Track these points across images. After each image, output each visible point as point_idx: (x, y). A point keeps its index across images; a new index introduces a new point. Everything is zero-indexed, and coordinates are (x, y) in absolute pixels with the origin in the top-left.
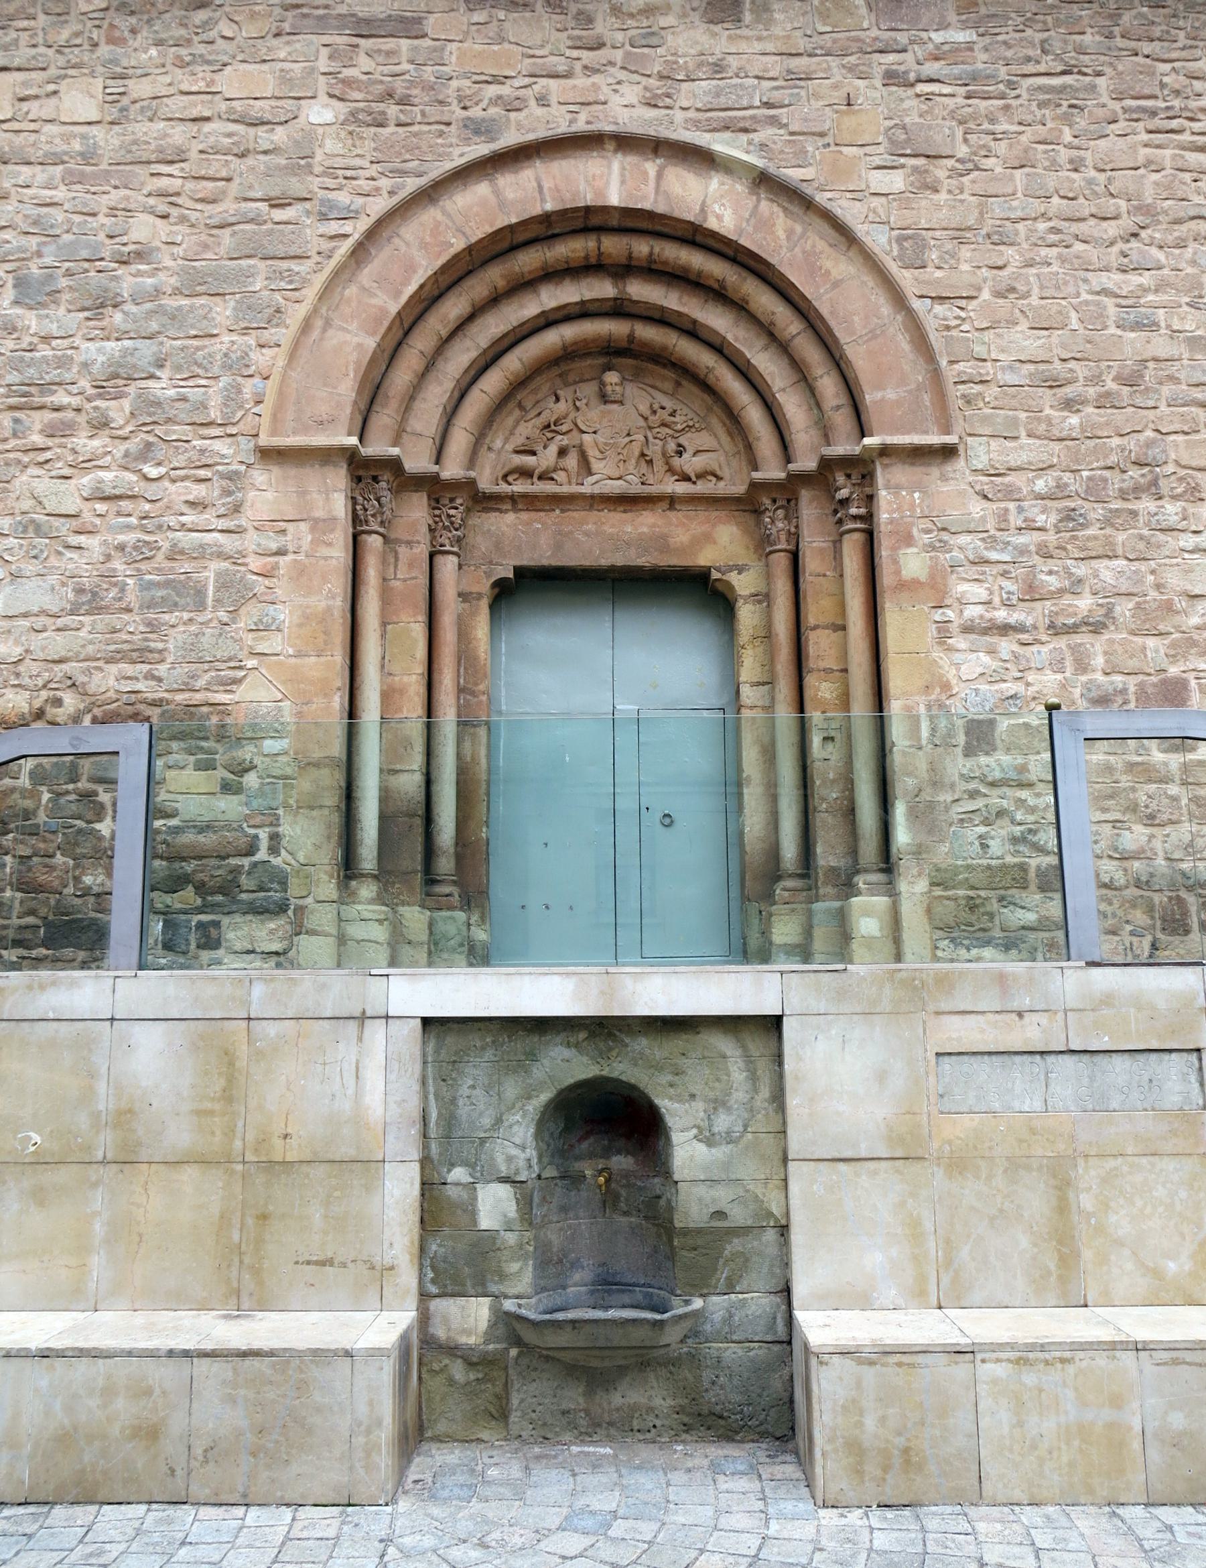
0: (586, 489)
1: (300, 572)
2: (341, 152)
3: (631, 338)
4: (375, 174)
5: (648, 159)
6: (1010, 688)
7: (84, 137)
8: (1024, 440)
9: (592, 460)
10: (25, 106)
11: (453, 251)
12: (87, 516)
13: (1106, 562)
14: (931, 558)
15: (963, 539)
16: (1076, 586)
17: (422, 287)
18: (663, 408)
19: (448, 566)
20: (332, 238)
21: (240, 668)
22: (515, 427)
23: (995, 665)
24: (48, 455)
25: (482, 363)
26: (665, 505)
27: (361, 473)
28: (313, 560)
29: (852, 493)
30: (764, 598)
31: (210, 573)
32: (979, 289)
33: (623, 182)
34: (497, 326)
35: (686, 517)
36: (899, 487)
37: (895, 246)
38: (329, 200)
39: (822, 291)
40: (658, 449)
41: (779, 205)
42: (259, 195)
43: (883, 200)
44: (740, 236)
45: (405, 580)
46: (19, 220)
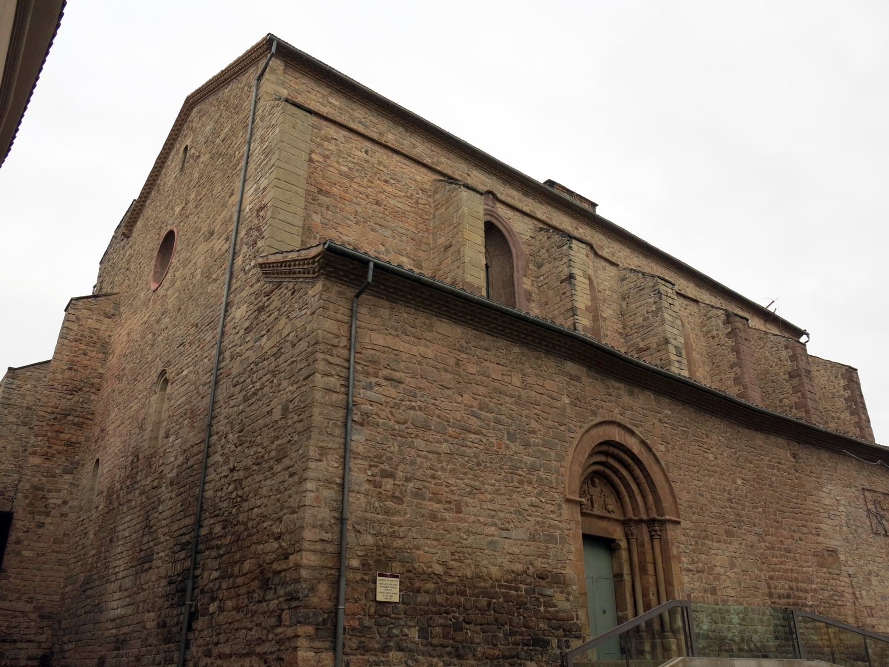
24: (519, 490)
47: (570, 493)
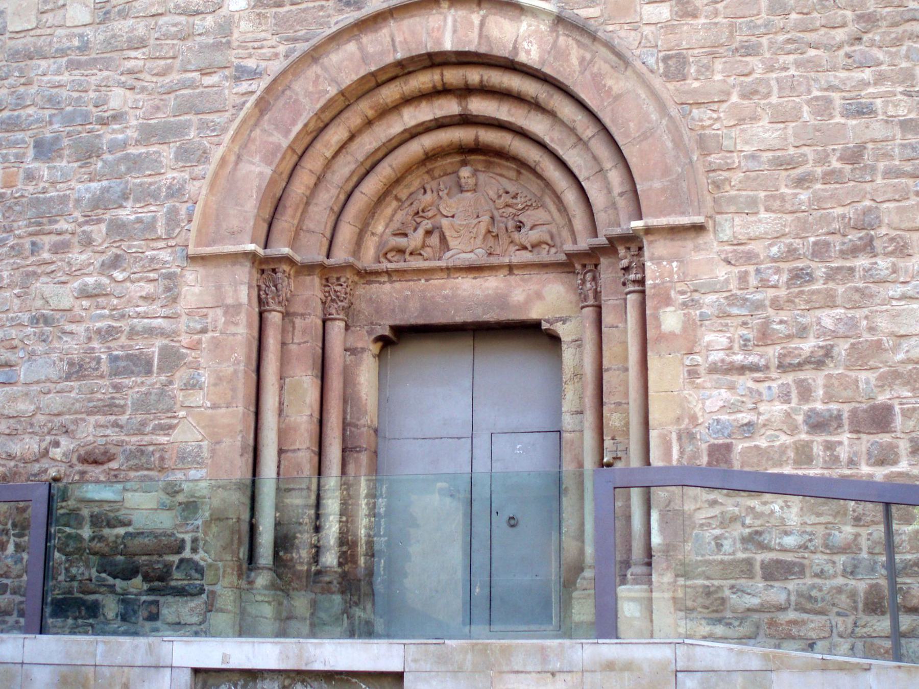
0: (442, 264)
1: (216, 344)
2: (252, 29)
3: (476, 140)
4: (274, 43)
5: (474, 12)
6: (745, 417)
7: (81, 36)
8: (763, 215)
9: (449, 239)
10: (44, 17)
11: (328, 96)
12: (77, 310)
13: (827, 311)
14: (685, 314)
15: (710, 298)
16: (802, 332)
17: (306, 125)
18: (507, 193)
19: (336, 329)
20: (243, 94)
21: (174, 417)
22: (393, 215)
23: (733, 398)
24: (53, 267)
25: (362, 170)
26: (506, 272)
27: (264, 267)
28: (225, 337)
29: (631, 263)
30: (578, 342)
31: (154, 348)
32: (729, 94)
33: (455, 31)
34: (370, 143)
35: (523, 280)
36: (661, 258)
37: (661, 65)
38: (241, 67)
39: (606, 104)
40: (502, 225)
41: (574, 39)
42: (193, 68)
43: (653, 28)
44: (543, 65)
45: (299, 344)
46: (38, 100)
47: (198, 244)
